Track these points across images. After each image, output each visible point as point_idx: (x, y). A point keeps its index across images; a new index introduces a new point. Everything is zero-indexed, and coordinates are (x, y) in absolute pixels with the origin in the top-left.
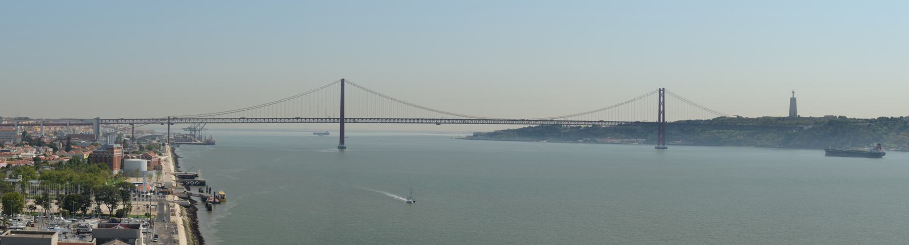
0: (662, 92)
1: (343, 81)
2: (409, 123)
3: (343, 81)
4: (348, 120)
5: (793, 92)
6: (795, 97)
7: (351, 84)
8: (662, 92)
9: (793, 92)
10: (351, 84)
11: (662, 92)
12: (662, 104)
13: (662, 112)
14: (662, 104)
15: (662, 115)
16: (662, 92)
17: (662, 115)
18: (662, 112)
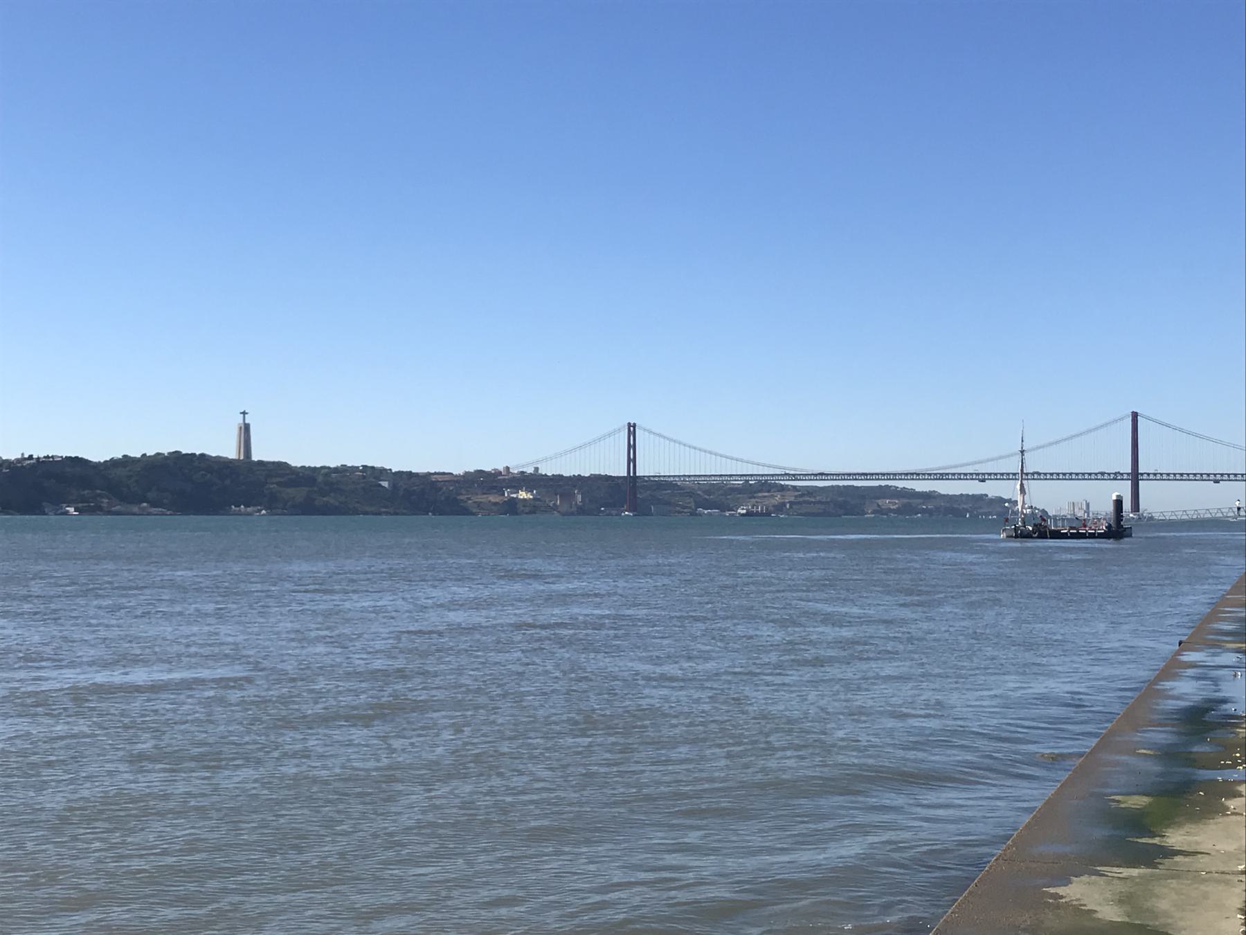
0: (632, 428)
1: (1135, 416)
2: (1089, 479)
3: (1135, 416)
4: (1145, 477)
5: (244, 413)
6: (247, 422)
7: (1148, 419)
8: (632, 429)
9: (244, 413)
10: (1148, 419)
11: (632, 429)
12: (632, 447)
13: (632, 461)
14: (632, 447)
15: (632, 464)
16: (632, 428)
17: (632, 464)
18: (632, 461)
